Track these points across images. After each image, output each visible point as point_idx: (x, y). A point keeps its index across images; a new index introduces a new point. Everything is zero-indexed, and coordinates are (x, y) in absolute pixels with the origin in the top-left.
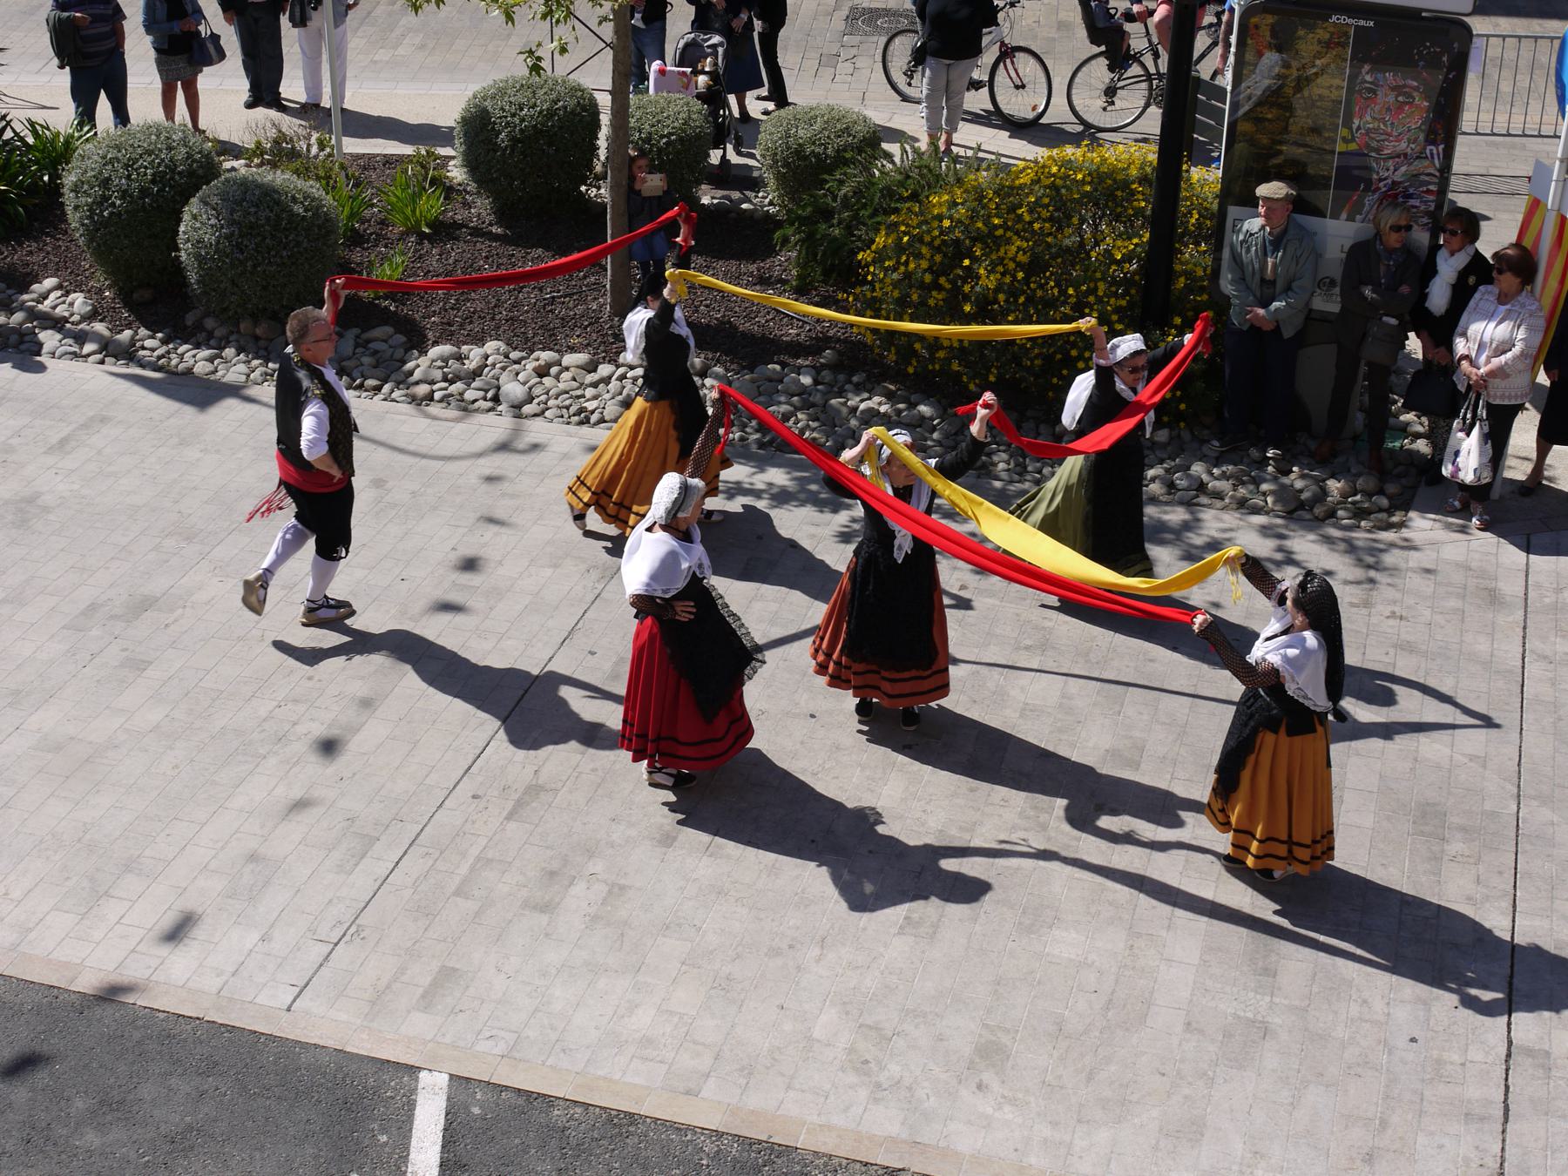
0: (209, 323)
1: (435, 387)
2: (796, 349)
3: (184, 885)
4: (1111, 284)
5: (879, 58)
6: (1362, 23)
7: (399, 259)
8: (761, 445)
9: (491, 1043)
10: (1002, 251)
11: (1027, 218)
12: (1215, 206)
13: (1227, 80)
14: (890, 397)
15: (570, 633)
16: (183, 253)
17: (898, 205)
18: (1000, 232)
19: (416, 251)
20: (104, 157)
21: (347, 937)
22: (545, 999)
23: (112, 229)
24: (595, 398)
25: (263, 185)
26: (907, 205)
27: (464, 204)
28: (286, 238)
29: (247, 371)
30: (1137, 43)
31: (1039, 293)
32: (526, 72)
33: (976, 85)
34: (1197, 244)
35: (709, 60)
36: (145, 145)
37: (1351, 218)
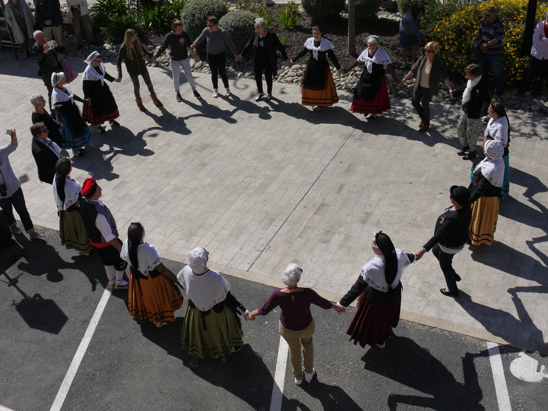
1: (294, 78)
9: (308, 283)
15: (335, 156)
19: (288, 35)
20: (193, 7)
22: (325, 270)
23: (196, 30)
24: (344, 81)
27: (303, 19)
36: (205, 3)
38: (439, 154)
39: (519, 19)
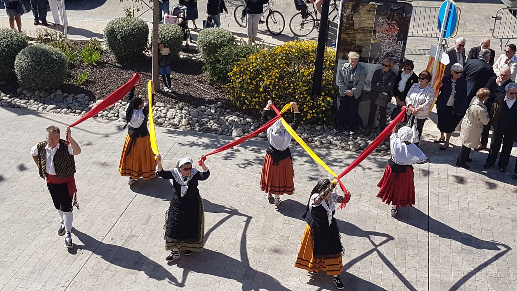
0: (25, 92)
2: (210, 102)
3: (17, 270)
4: (303, 83)
5: (233, 14)
6: (379, 4)
7: (86, 73)
8: (200, 131)
10: (271, 72)
11: (279, 63)
12: (334, 60)
13: (338, 21)
14: (238, 116)
16: (16, 70)
17: (240, 59)
18: (270, 67)
19: (92, 71)
21: (71, 285)
25: (42, 49)
26: (243, 59)
28: (50, 66)
29: (37, 107)
30: (310, 10)
31: (282, 85)
32: (126, 16)
33: (262, 22)
34: (329, 70)
35: (182, 13)
37: (375, 63)
38: (242, 184)
39: (309, 61)
